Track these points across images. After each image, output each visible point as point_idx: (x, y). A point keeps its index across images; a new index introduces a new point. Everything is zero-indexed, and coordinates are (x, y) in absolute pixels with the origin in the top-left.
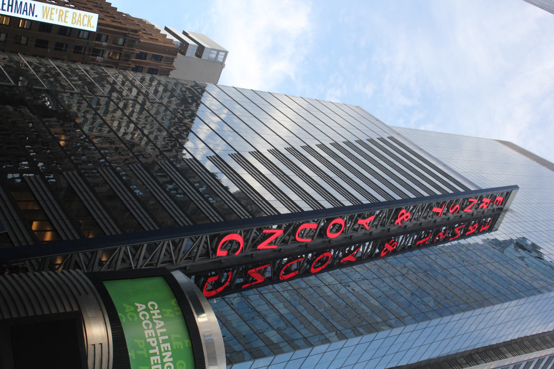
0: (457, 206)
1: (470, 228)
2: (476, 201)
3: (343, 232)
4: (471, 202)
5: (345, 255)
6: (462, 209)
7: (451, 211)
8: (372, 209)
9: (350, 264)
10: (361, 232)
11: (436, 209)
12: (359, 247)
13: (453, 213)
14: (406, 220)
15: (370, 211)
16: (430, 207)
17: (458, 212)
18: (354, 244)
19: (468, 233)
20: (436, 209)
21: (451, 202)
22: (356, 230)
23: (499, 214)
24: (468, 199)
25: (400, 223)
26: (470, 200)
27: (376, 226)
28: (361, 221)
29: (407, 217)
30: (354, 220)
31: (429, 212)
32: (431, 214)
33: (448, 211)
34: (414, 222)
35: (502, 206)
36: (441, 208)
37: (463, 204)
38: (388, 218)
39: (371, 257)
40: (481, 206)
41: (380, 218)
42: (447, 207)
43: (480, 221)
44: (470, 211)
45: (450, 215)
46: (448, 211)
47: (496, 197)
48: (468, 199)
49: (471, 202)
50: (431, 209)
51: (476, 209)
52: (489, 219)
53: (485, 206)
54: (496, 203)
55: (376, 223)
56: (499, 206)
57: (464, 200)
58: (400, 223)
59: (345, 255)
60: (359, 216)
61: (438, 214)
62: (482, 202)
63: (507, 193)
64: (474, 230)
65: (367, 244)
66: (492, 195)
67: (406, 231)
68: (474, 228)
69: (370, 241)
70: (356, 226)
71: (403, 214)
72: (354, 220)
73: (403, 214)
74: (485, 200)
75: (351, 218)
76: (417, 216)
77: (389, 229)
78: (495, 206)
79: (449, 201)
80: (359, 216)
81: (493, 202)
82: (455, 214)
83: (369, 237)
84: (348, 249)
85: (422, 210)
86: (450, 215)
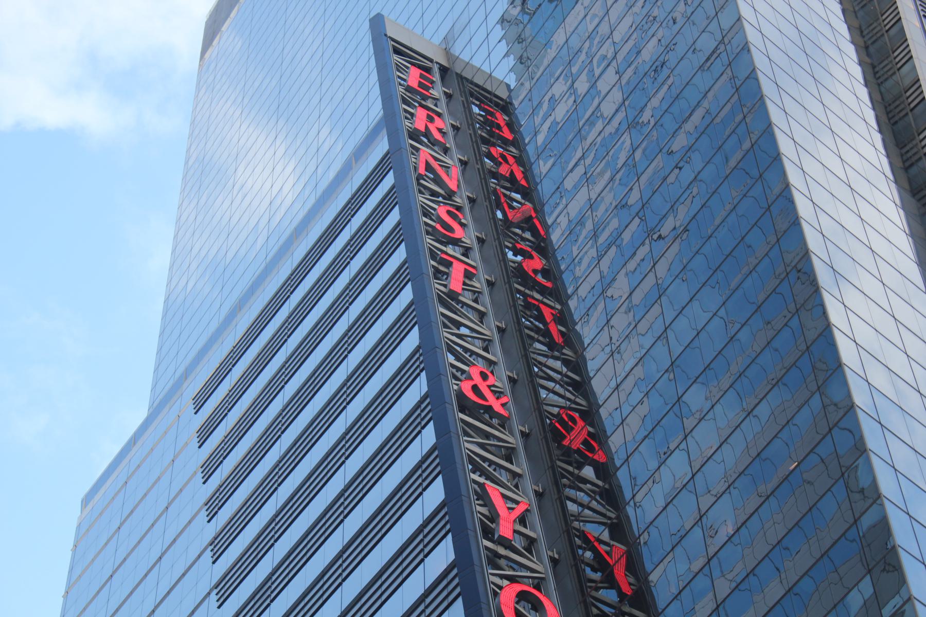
0: (442, 211)
1: (504, 170)
2: (426, 152)
3: (537, 587)
4: (428, 168)
5: (610, 581)
6: (450, 195)
7: (458, 233)
8: (464, 492)
9: (634, 565)
10: (536, 530)
11: (456, 281)
12: (584, 536)
13: (463, 225)
14: (491, 380)
15: (473, 497)
16: (450, 299)
17: (459, 208)
18: (573, 548)
19: (519, 176)
20: (456, 281)
21: (431, 232)
22: (531, 543)
23: (460, 77)
24: (419, 177)
25: (504, 400)
26: (422, 170)
27: (515, 475)
28: (505, 529)
29: (484, 376)
30: (501, 551)
31: (464, 304)
32: (467, 298)
33: (456, 242)
34: (496, 354)
35: (436, 69)
36: (448, 264)
37: (434, 194)
38: (488, 436)
39: (611, 496)
40: (437, 136)
41: (484, 459)
42: (445, 244)
43: (485, 141)
44: (456, 171)
45: (469, 237)
46: (456, 242)
47: (409, 89)
48: (419, 177)
49: (428, 168)
50: (453, 295)
51: (446, 151)
52: (476, 110)
53: (438, 122)
54: (427, 89)
55: (504, 477)
56: (436, 77)
57: (422, 189)
58: (504, 400)
59: (610, 581)
60: (488, 533)
61: (468, 275)
62: (427, 134)
63: (397, 51)
64: (511, 160)
65: (572, 507)
66: (405, 101)
67: (526, 381)
68: (503, 157)
69: (562, 501)
70: (518, 543)
71: (475, 388)
72: (501, 551)
73: (475, 388)
74: (420, 123)
75: (494, 559)
76: (479, 343)
77: (523, 434)
78: (437, 91)
79: (429, 240)
80: (488, 533)
81: (425, 98)
82: (467, 219)
83: (552, 496)
84: (588, 570)
85: (458, 325)
86: (469, 237)
